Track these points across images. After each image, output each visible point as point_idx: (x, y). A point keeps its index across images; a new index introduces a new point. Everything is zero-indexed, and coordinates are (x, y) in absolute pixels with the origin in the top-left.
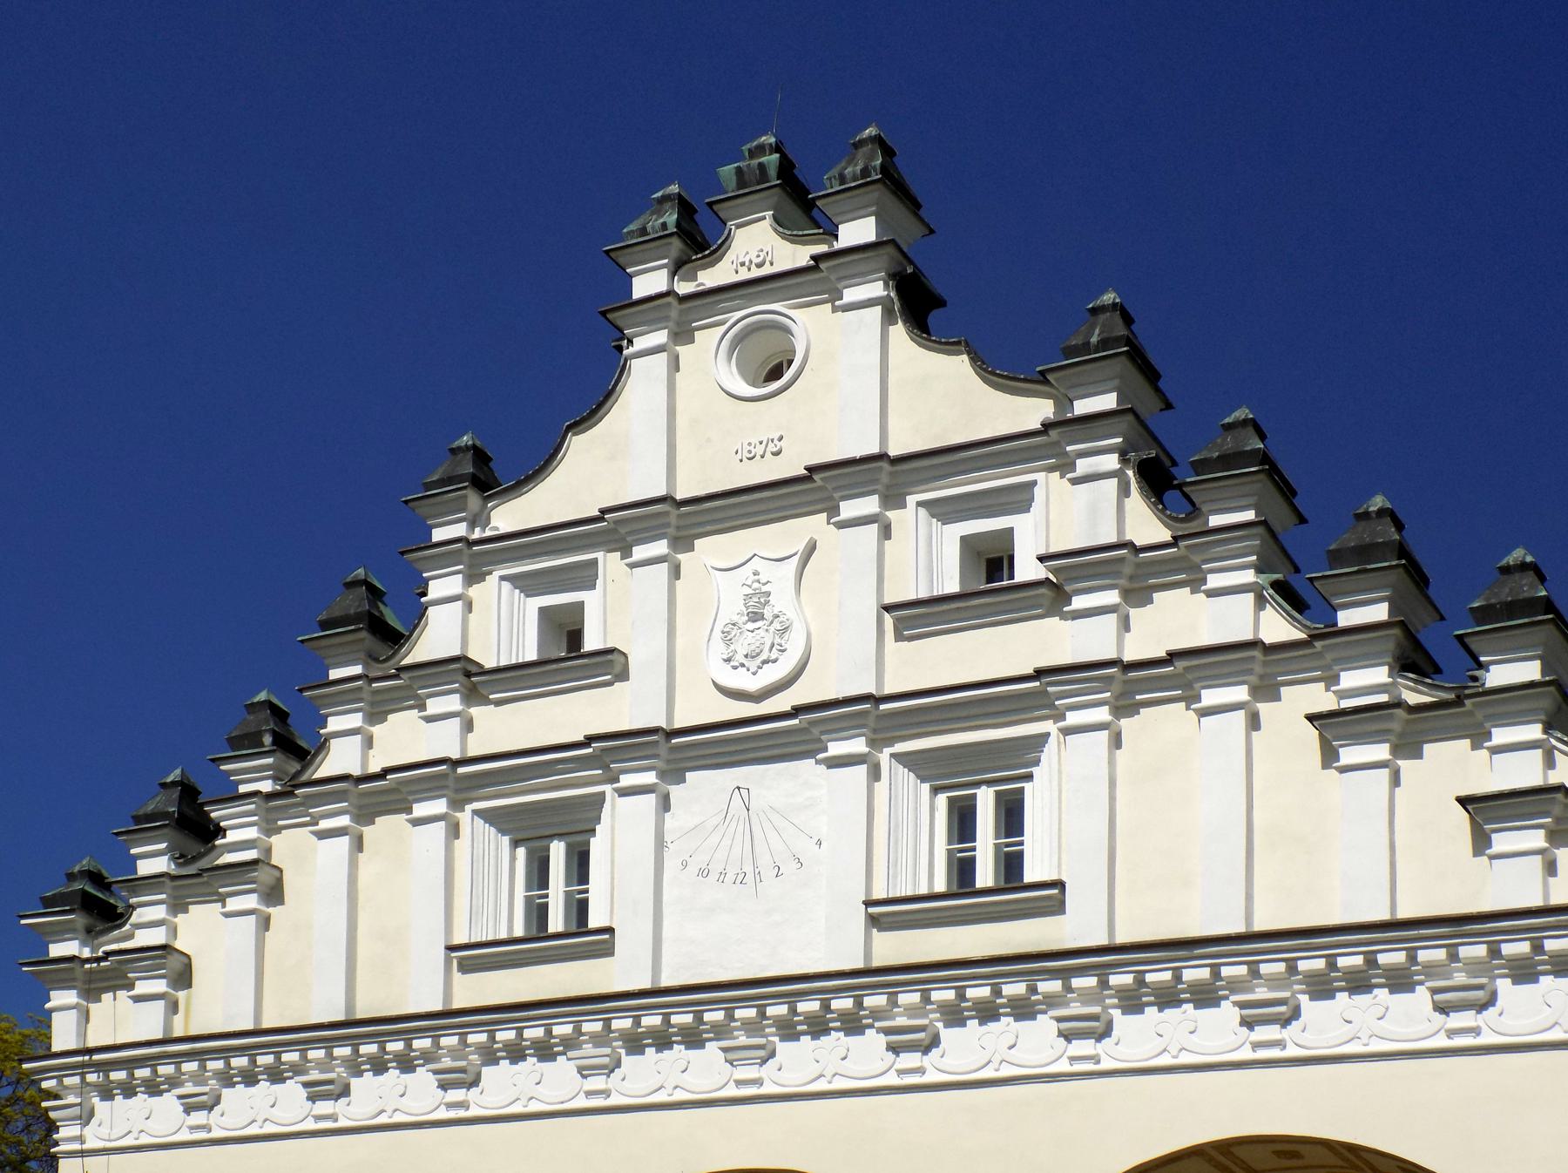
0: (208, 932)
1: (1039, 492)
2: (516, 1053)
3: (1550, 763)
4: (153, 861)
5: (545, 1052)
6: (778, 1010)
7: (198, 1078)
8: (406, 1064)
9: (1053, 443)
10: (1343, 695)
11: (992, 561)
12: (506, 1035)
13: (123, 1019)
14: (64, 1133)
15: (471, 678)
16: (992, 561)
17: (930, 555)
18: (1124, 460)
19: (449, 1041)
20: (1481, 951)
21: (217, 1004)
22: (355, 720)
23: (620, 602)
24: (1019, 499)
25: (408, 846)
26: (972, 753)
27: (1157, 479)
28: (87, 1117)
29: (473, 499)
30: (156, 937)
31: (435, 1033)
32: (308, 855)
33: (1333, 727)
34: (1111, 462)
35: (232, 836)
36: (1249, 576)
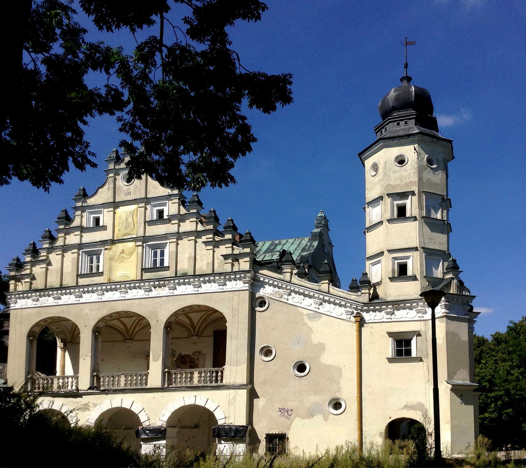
0: (38, 270)
1: (167, 204)
2: (88, 292)
3: (233, 249)
4: (28, 259)
5: (93, 292)
6: (128, 286)
7: (36, 296)
8: (70, 294)
9: (169, 197)
10: (207, 238)
11: (161, 213)
12: (86, 289)
13: (22, 287)
14: (11, 305)
15: (82, 229)
16: (161, 213)
17: (152, 213)
18: (179, 200)
19: (77, 290)
20: (223, 277)
21: (38, 284)
22: (63, 235)
23: (106, 217)
24: (165, 204)
25: (70, 256)
26: (152, 244)
27: (183, 202)
28: (16, 302)
29: (83, 199)
30: (28, 272)
31: (74, 289)
32: (55, 258)
33: (205, 243)
34: (177, 201)
35: (42, 254)
36: (195, 219)
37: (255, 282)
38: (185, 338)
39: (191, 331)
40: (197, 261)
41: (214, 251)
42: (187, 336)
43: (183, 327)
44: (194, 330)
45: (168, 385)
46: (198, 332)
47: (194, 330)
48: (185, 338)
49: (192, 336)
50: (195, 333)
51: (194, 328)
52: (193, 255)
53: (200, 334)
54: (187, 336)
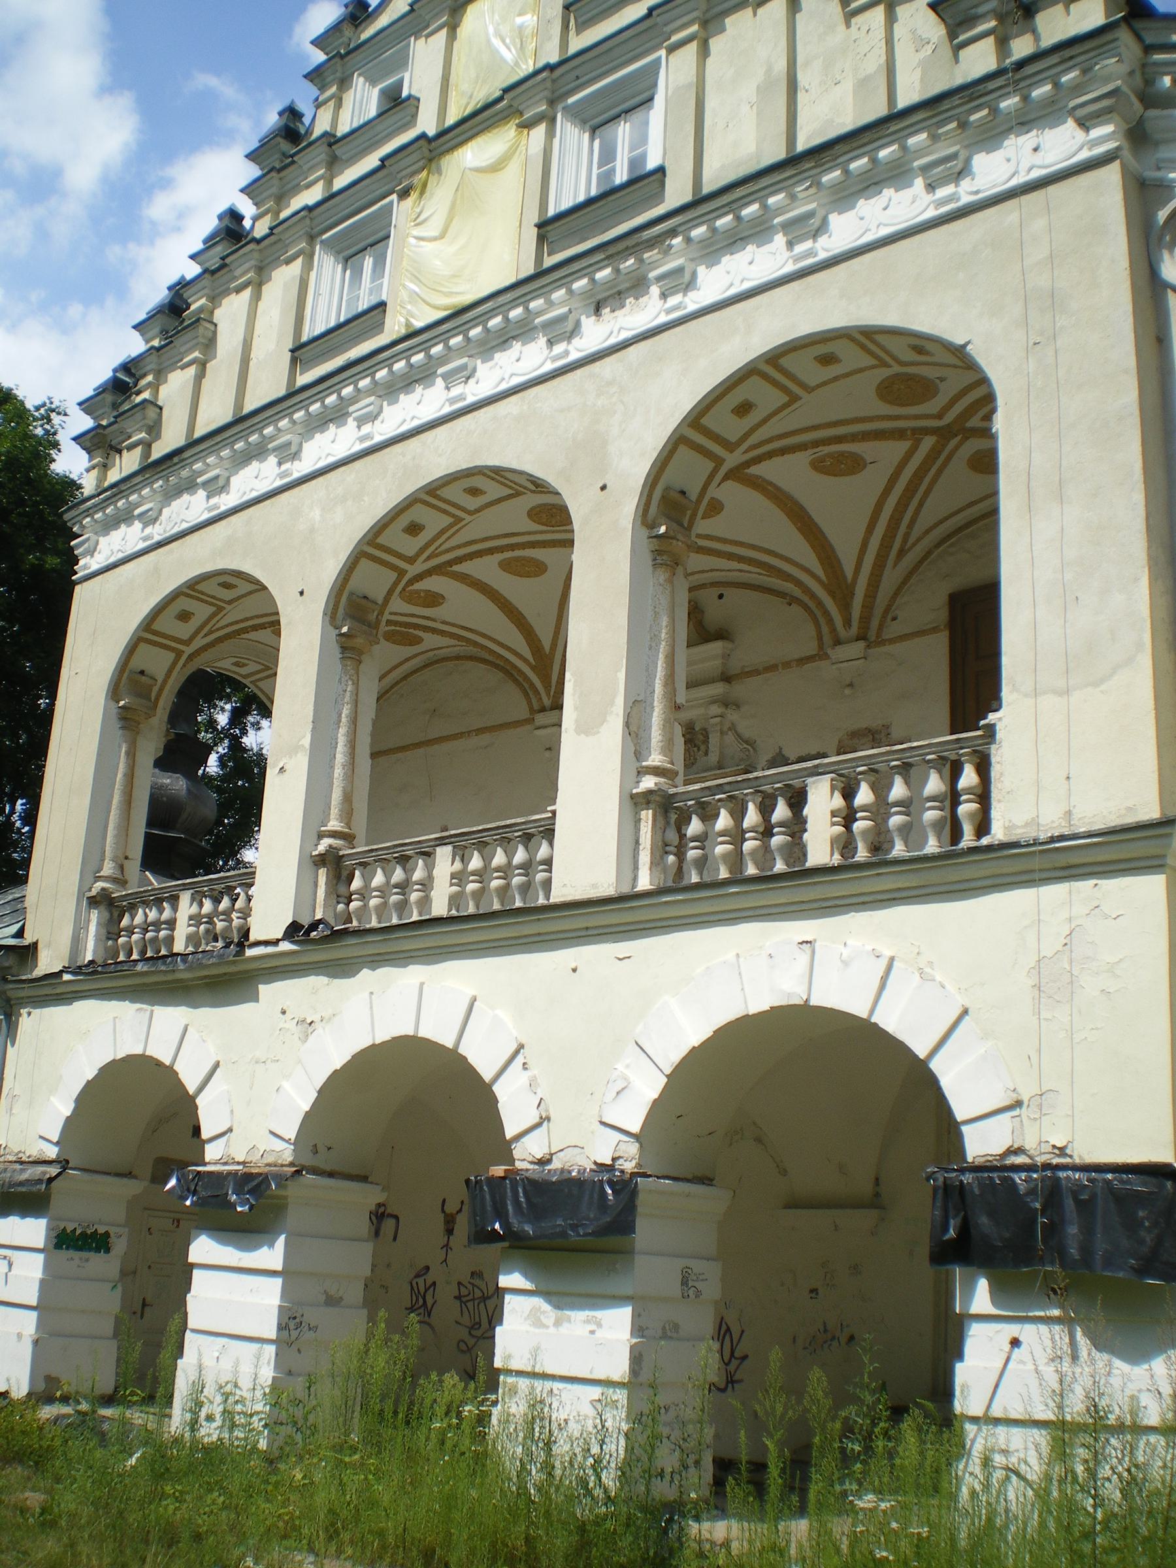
37: (1152, 113)
38: (802, 661)
39: (830, 621)
40: (801, 97)
41: (891, 18)
42: (811, 648)
43: (792, 600)
44: (845, 606)
45: (676, 899)
46: (865, 620)
47: (845, 606)
48: (802, 661)
49: (838, 642)
50: (848, 623)
51: (841, 590)
52: (781, 65)
53: (875, 623)
54: (811, 648)
